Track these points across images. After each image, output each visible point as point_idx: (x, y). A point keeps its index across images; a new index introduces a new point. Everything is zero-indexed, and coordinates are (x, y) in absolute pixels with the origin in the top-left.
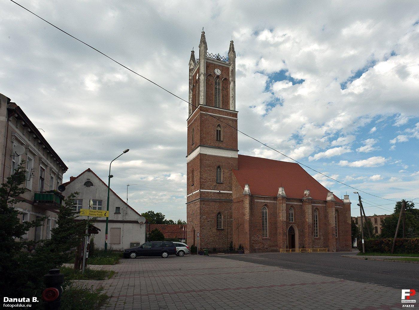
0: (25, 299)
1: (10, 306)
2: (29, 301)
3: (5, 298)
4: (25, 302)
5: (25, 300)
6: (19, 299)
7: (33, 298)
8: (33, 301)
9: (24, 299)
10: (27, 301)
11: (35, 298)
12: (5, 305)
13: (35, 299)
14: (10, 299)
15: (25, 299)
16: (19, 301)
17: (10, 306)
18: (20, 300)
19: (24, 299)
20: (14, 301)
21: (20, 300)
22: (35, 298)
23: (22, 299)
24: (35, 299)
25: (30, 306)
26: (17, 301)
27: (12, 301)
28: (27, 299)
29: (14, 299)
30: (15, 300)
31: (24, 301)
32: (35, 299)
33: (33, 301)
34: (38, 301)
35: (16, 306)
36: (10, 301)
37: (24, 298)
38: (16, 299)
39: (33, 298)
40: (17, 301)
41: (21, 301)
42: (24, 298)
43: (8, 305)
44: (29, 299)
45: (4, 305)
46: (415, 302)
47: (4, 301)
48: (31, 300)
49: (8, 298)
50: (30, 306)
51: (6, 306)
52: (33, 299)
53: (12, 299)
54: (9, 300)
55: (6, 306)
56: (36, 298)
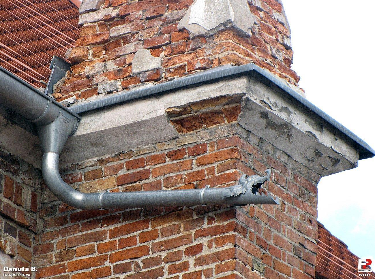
0: (24, 268)
1: (10, 275)
2: (28, 271)
3: (4, 267)
4: (24, 271)
5: (24, 269)
6: (19, 268)
7: (32, 267)
9: (23, 268)
11: (33, 268)
12: (5, 275)
13: (33, 269)
14: (10, 268)
15: (24, 268)
17: (10, 275)
18: (20, 269)
19: (23, 268)
20: (13, 271)
21: (20, 269)
22: (33, 268)
23: (21, 268)
25: (29, 275)
28: (26, 268)
29: (14, 269)
31: (23, 270)
32: (33, 269)
34: (37, 271)
35: (15, 275)
37: (23, 267)
38: (16, 269)
39: (32, 267)
40: (16, 271)
41: (21, 270)
42: (23, 267)
44: (28, 269)
49: (7, 268)
50: (29, 275)
52: (32, 269)
53: (11, 269)
54: (9, 269)
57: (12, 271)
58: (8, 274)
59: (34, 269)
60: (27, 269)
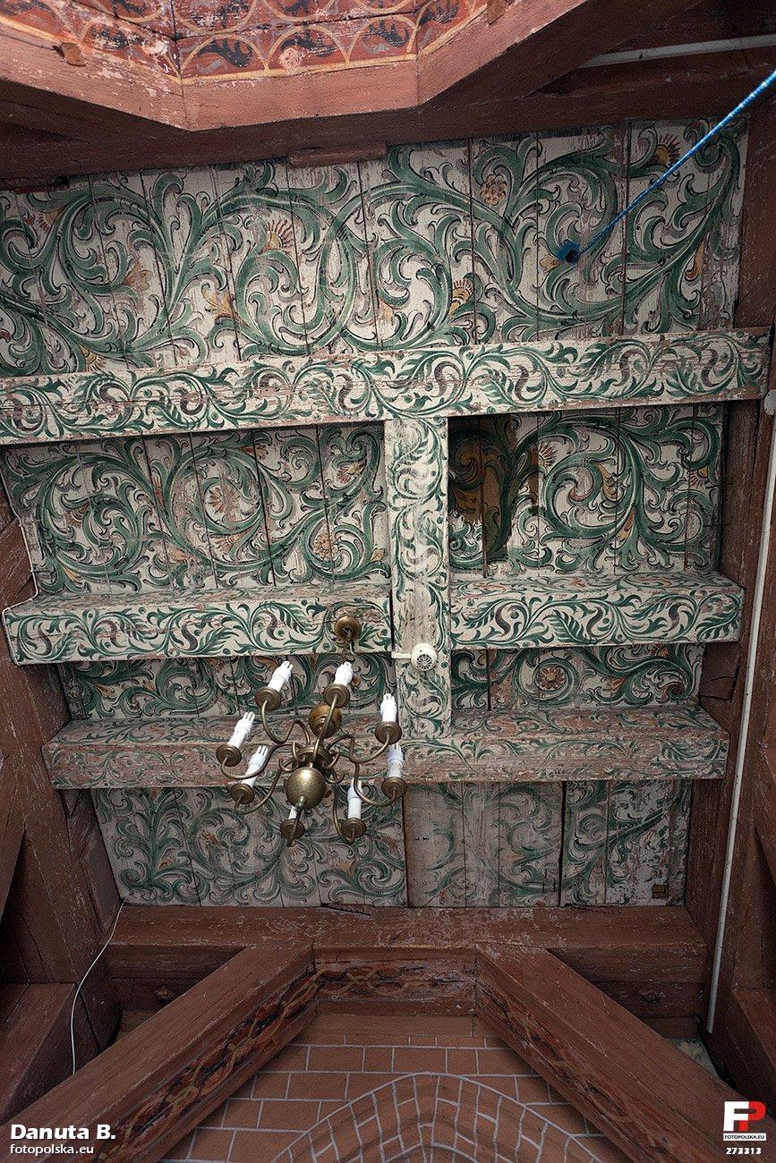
0: (75, 1129)
1: (31, 1150)
2: (87, 1137)
4: (74, 1138)
5: (75, 1133)
6: (57, 1130)
7: (100, 1127)
8: (99, 1137)
9: (72, 1129)
10: (80, 1136)
11: (103, 1129)
12: (14, 1149)
13: (103, 1131)
14: (30, 1130)
16: (58, 1136)
17: (31, 1150)
18: (61, 1133)
19: (72, 1129)
20: (42, 1137)
21: (61, 1133)
22: (103, 1129)
23: (65, 1130)
24: (104, 1132)
26: (50, 1137)
27: (36, 1137)
29: (43, 1131)
30: (46, 1134)
32: (103, 1131)
33: (99, 1137)
36: (29, 1136)
37: (72, 1127)
39: (100, 1127)
40: (50, 1137)
41: (64, 1136)
42: (72, 1127)
43: (25, 1147)
44: (86, 1132)
45: (12, 1147)
46: (765, 1139)
47: (13, 1136)
48: (93, 1132)
51: (19, 1150)
52: (100, 1131)
53: (35, 1131)
55: (19, 1150)
56: (108, 1127)
57: (36, 1137)
58: (25, 1147)
59: (106, 1131)
60: (85, 1133)
